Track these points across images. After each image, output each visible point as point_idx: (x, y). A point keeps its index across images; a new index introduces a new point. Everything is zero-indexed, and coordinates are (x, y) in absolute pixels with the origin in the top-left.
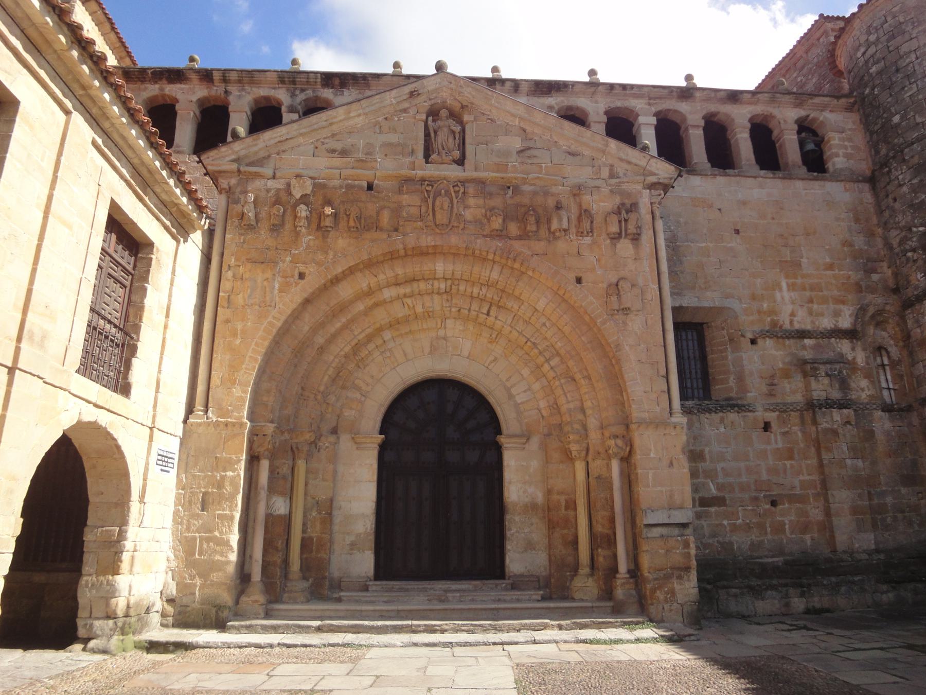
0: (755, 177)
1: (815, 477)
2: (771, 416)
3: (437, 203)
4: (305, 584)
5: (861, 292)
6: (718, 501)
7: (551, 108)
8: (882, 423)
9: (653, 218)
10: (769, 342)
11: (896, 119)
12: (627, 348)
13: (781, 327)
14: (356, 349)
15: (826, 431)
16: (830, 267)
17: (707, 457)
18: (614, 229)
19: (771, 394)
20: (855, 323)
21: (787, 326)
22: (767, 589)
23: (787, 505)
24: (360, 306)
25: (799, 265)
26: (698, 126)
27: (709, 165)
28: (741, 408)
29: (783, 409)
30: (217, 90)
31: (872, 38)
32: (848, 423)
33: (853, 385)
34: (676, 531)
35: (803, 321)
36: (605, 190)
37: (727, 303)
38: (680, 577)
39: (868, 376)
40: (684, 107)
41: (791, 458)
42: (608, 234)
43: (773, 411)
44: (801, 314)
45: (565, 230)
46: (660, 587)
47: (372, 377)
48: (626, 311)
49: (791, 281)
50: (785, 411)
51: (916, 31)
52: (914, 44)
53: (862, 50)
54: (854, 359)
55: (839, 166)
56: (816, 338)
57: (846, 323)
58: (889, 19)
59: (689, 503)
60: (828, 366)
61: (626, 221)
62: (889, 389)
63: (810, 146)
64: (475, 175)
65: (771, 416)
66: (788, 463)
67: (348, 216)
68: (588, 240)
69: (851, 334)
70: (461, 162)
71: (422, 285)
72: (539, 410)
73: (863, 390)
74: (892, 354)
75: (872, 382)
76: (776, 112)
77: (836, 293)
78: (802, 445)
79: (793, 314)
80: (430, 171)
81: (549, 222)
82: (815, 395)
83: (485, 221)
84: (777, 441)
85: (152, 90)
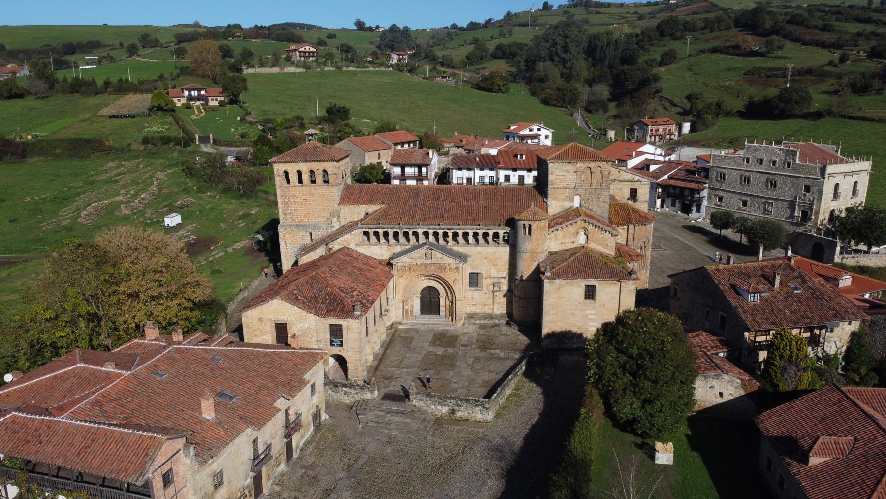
35: (496, 275)
57: (504, 276)
69: (505, 278)
80: (426, 261)
84: (487, 295)
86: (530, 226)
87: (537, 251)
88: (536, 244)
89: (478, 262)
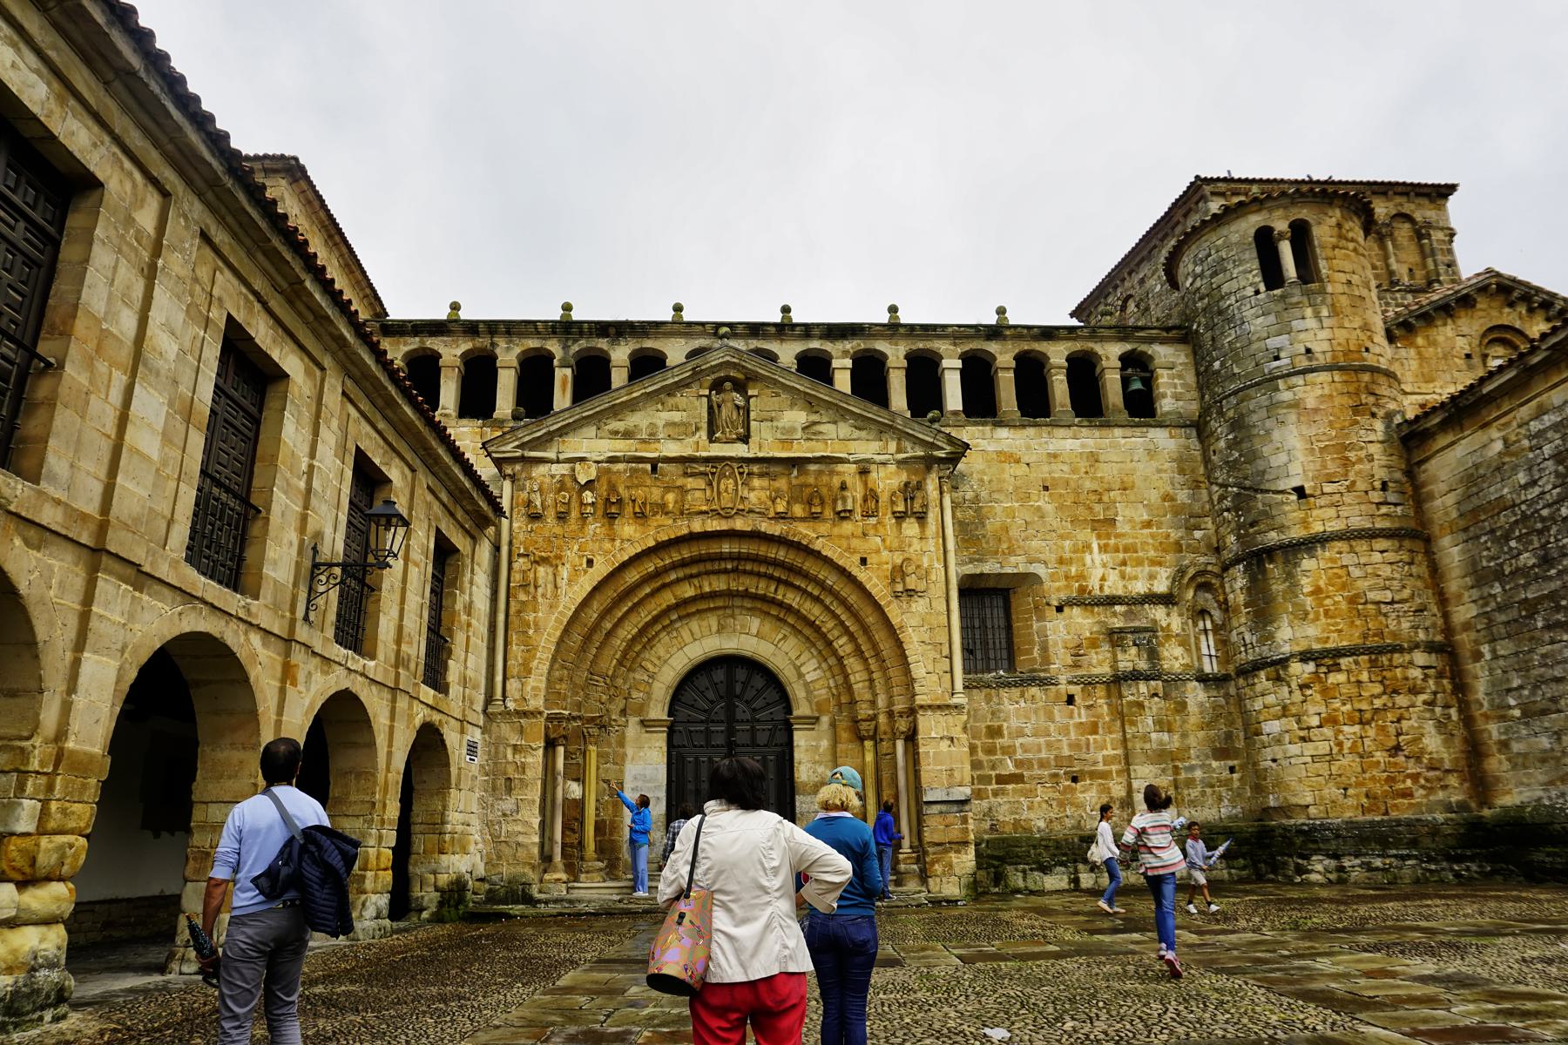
0: (1069, 426)
1: (1119, 752)
2: (1075, 690)
3: (722, 487)
4: (600, 864)
5: (1181, 551)
6: (1016, 778)
7: (845, 353)
8: (1196, 695)
9: (941, 493)
10: (1076, 611)
11: (1217, 365)
12: (910, 630)
13: (1090, 593)
14: (642, 631)
15: (1131, 704)
16: (1148, 524)
17: (1005, 732)
18: (901, 508)
19: (1076, 666)
20: (1171, 588)
21: (1097, 592)
22: (1055, 865)
23: (1088, 782)
24: (648, 590)
25: (1112, 522)
26: (1008, 369)
27: (1019, 414)
28: (1044, 683)
29: (1088, 683)
30: (483, 342)
31: (1198, 269)
32: (1156, 695)
33: (1166, 654)
34: (955, 808)
35: (1114, 586)
36: (892, 468)
37: (1032, 569)
38: (958, 852)
39: (1184, 643)
40: (993, 347)
41: (1096, 733)
42: (894, 513)
43: (1076, 683)
44: (1113, 577)
45: (850, 511)
46: (938, 861)
47: (659, 658)
48: (910, 593)
49: (1102, 542)
50: (1090, 683)
51: (1236, 271)
52: (1234, 285)
53: (1190, 280)
54: (1169, 625)
55: (1166, 409)
56: (1127, 604)
57: (1161, 587)
58: (1213, 252)
59: (968, 779)
60: (1137, 635)
61: (912, 499)
62: (1210, 656)
63: (1137, 385)
64: (761, 455)
65: (1075, 690)
66: (1091, 738)
67: (634, 501)
68: (873, 521)
69: (1167, 600)
70: (745, 439)
71: (709, 566)
72: (830, 688)
73: (1176, 659)
74: (1215, 618)
75: (1188, 650)
76: (1098, 348)
77: (1152, 553)
78: (1107, 719)
79: (1103, 579)
80: (717, 450)
81: (835, 501)
82: (1121, 665)
83: (770, 503)
85: (413, 343)
86: (1301, 235)
87: (1370, 360)
88: (1357, 323)
89: (1011, 513)
